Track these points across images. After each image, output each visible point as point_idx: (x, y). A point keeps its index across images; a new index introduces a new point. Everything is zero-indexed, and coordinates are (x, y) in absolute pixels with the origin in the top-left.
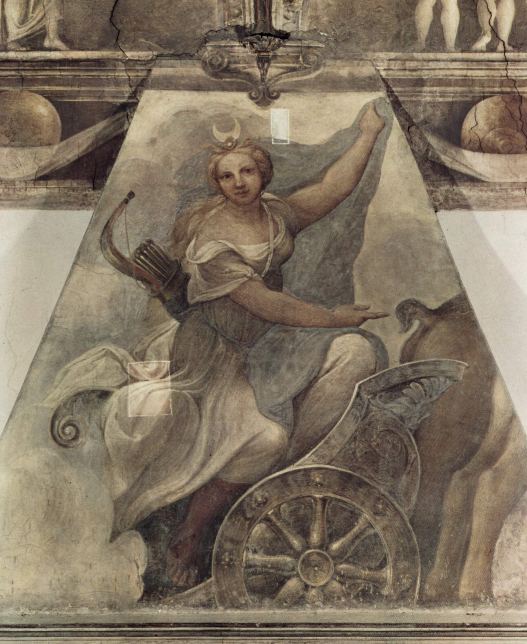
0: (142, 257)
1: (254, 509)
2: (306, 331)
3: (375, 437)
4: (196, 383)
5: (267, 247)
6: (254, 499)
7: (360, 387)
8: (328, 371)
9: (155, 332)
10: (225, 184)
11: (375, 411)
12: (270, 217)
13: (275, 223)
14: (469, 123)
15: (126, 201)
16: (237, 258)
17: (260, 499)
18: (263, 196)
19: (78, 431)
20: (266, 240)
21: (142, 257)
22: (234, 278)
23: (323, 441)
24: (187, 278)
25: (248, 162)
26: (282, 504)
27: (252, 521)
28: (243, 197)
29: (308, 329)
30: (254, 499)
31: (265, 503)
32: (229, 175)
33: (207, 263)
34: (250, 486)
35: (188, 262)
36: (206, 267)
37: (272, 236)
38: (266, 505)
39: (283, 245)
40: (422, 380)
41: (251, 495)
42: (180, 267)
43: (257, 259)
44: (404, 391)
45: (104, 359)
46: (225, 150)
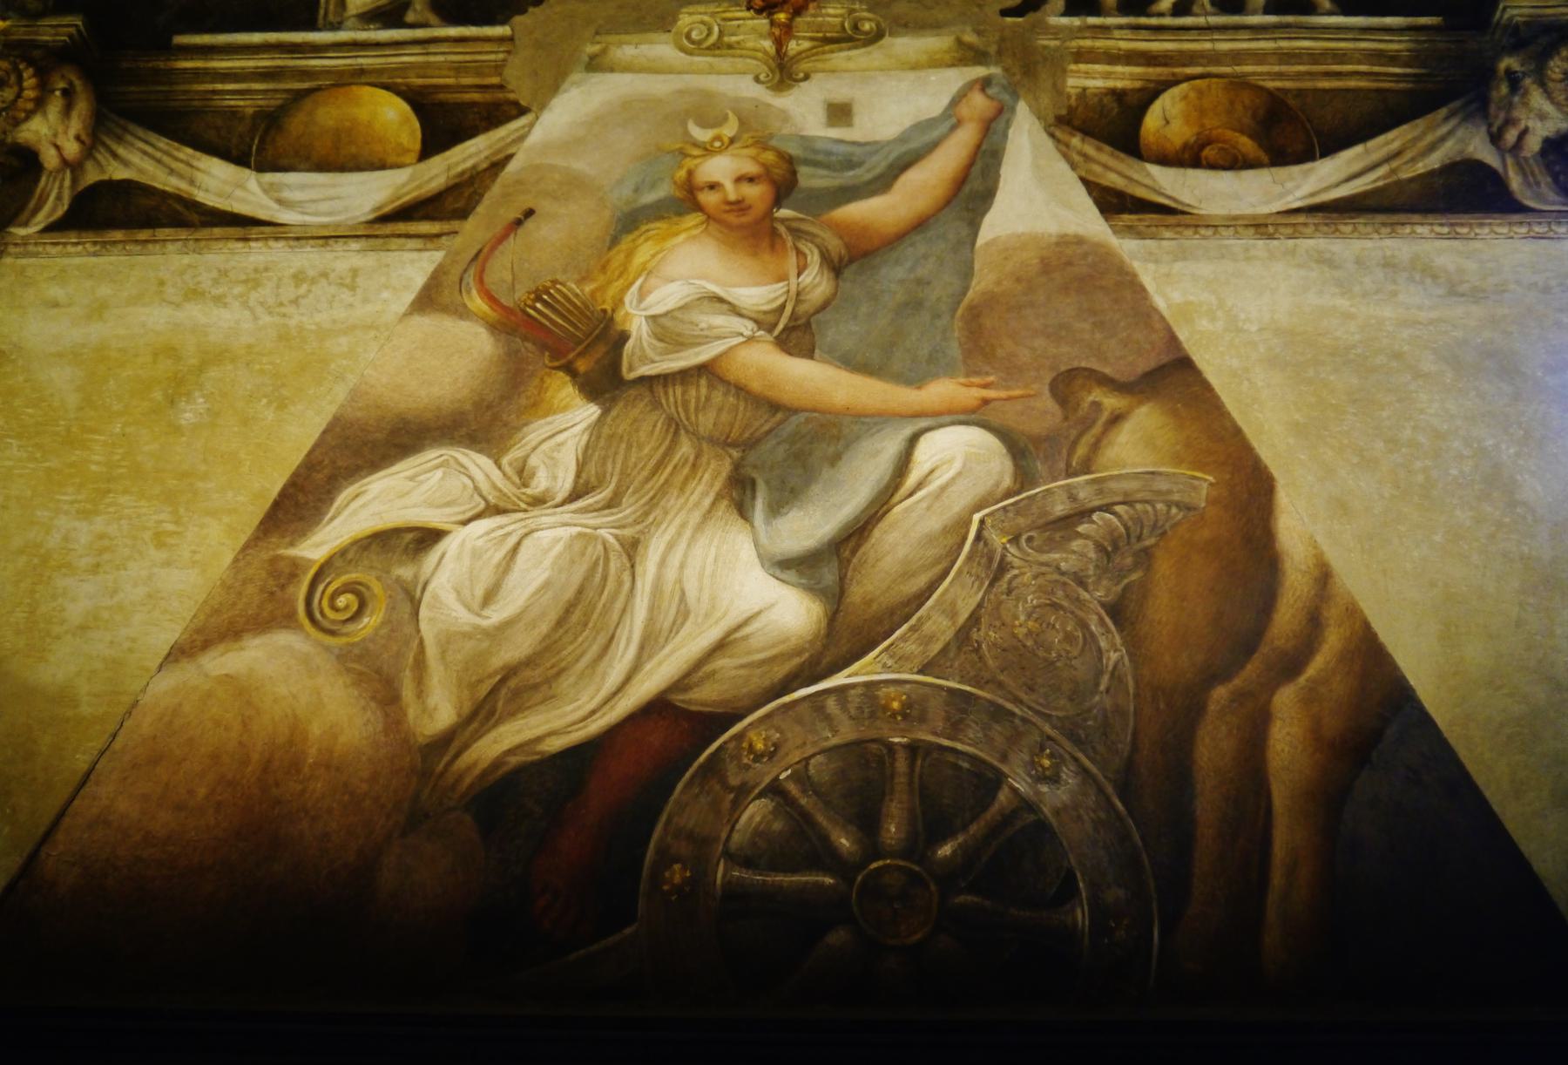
0: (539, 305)
1: (747, 767)
2: (863, 423)
3: (1022, 618)
4: (626, 517)
5: (785, 289)
6: (745, 745)
7: (982, 522)
8: (911, 494)
9: (551, 427)
10: (709, 199)
11: (1019, 568)
12: (789, 244)
13: (799, 253)
14: (1152, 121)
15: (518, 223)
16: (725, 307)
17: (760, 746)
18: (777, 215)
19: (362, 605)
20: (782, 278)
21: (539, 305)
22: (719, 338)
23: (905, 627)
24: (624, 337)
25: (751, 168)
26: (813, 755)
27: (742, 793)
28: (738, 216)
29: (867, 420)
30: (745, 745)
31: (772, 755)
32: (713, 186)
33: (666, 314)
34: (741, 717)
35: (627, 314)
36: (663, 321)
37: (793, 272)
38: (775, 759)
39: (815, 286)
40: (1118, 508)
41: (740, 737)
42: (612, 319)
43: (765, 308)
44: (1081, 529)
45: (439, 473)
46: (708, 150)
